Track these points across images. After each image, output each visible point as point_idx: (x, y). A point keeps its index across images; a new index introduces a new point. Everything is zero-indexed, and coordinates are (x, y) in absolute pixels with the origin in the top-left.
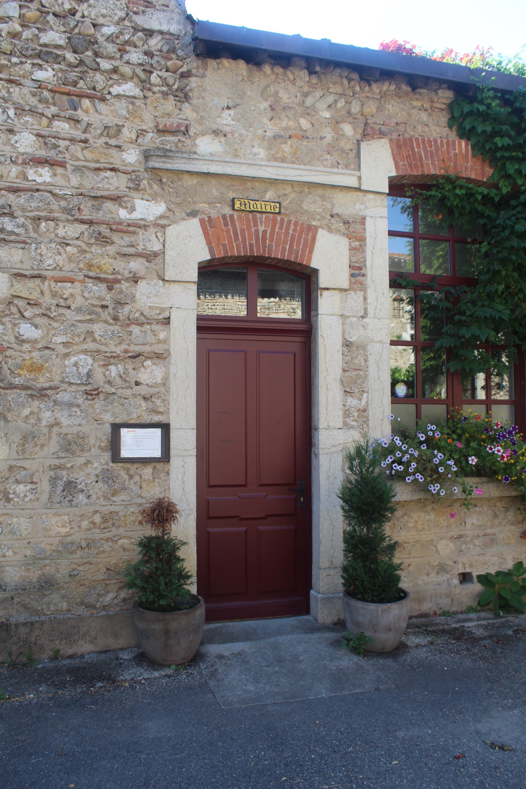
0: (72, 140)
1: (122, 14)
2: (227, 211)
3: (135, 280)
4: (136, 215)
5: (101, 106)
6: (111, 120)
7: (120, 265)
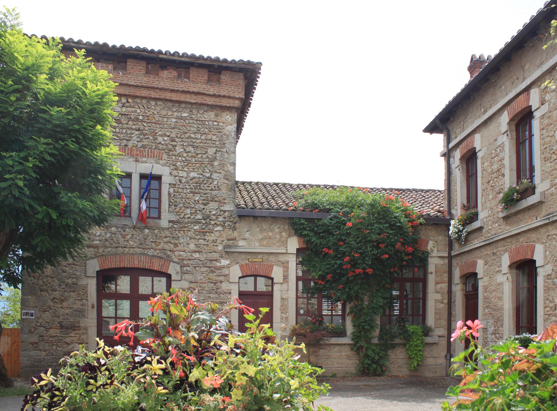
0: (204, 245)
1: (217, 207)
2: (247, 262)
3: (221, 282)
4: (222, 264)
5: (212, 234)
6: (214, 238)
7: (217, 278)
